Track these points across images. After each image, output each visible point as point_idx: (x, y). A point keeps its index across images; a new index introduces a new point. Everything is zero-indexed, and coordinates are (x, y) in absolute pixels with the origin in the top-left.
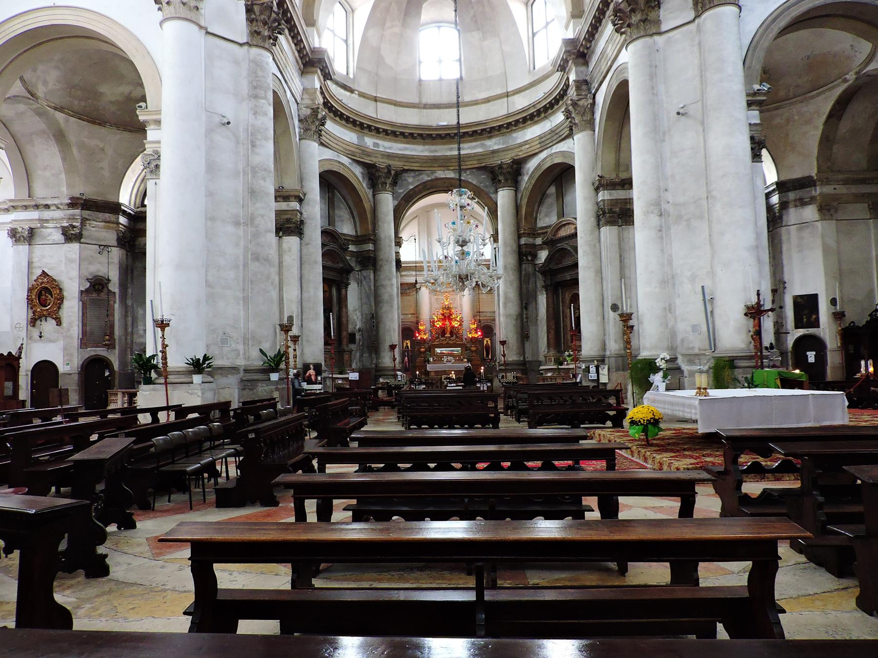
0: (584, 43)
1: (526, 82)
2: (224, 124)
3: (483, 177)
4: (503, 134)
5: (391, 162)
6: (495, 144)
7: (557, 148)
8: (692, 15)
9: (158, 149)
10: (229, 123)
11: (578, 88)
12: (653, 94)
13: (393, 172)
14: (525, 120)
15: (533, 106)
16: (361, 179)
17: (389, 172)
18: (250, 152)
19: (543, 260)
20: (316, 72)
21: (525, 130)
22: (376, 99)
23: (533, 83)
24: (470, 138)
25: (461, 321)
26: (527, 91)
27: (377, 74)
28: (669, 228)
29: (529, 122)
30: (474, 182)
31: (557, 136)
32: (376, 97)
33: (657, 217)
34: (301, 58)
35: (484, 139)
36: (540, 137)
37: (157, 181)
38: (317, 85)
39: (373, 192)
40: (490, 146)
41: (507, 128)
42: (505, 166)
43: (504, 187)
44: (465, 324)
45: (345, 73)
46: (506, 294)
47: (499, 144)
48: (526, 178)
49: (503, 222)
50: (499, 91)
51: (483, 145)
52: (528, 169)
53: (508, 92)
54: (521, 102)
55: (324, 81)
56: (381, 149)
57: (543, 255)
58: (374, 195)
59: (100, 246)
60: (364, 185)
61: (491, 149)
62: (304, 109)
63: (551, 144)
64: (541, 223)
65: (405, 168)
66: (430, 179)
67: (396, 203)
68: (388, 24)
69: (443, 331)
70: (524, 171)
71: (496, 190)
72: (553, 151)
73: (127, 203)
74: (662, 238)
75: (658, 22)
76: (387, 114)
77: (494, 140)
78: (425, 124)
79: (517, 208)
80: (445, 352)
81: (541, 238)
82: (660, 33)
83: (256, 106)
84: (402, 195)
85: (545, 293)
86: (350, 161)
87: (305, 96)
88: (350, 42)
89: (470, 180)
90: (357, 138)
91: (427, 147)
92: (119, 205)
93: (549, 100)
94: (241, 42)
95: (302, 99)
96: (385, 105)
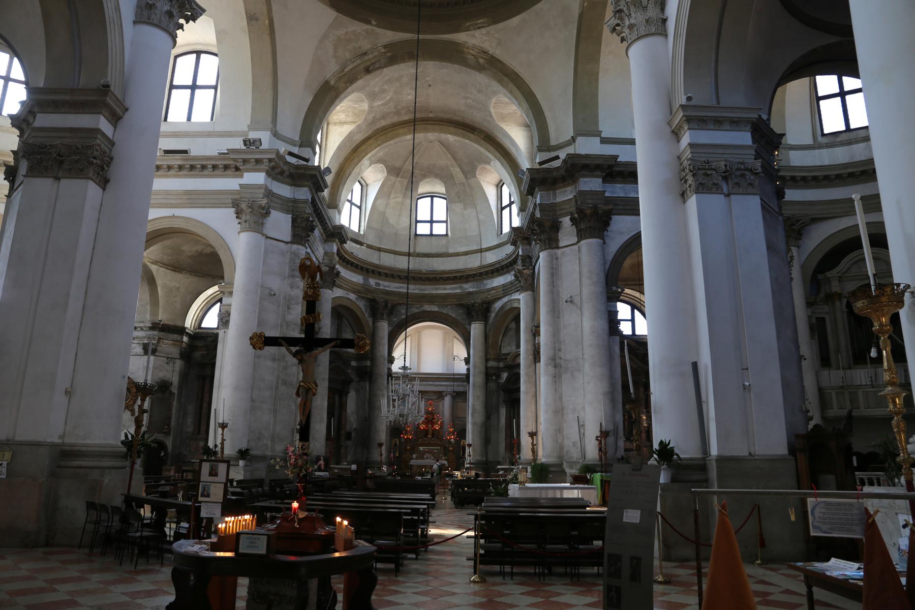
1: (495, 243)
2: (271, 295)
4: (477, 280)
5: (388, 298)
6: (470, 287)
7: (514, 296)
8: (576, 240)
9: (228, 310)
10: (274, 295)
11: (523, 261)
12: (553, 286)
13: (389, 305)
14: (492, 272)
16: (363, 310)
17: (386, 305)
18: (286, 312)
20: (335, 241)
21: (493, 279)
22: (379, 250)
23: (500, 245)
24: (452, 282)
26: (496, 250)
27: (382, 231)
28: (560, 376)
30: (453, 315)
31: (515, 287)
32: (380, 248)
33: (553, 368)
34: (325, 233)
35: (462, 283)
36: (503, 286)
37: (226, 330)
39: (373, 320)
40: (467, 289)
41: (480, 276)
43: (475, 321)
45: (357, 231)
47: (474, 287)
48: (493, 315)
49: (474, 349)
50: (475, 247)
51: (461, 288)
52: (495, 309)
53: (481, 249)
54: (491, 258)
55: (341, 245)
56: (381, 287)
57: (505, 375)
58: (374, 323)
60: (367, 315)
61: (467, 291)
62: (324, 267)
63: (511, 292)
64: (504, 351)
65: (400, 302)
66: (418, 311)
67: (391, 328)
68: (392, 196)
70: (492, 310)
71: (470, 322)
72: (512, 298)
74: (555, 382)
75: (557, 241)
76: (387, 260)
77: (469, 284)
78: (417, 269)
79: (486, 337)
82: (558, 248)
83: (292, 282)
84: (396, 323)
86: (356, 297)
88: (363, 208)
89: (450, 314)
90: (363, 279)
91: (418, 286)
93: (509, 260)
94: (286, 240)
95: (323, 259)
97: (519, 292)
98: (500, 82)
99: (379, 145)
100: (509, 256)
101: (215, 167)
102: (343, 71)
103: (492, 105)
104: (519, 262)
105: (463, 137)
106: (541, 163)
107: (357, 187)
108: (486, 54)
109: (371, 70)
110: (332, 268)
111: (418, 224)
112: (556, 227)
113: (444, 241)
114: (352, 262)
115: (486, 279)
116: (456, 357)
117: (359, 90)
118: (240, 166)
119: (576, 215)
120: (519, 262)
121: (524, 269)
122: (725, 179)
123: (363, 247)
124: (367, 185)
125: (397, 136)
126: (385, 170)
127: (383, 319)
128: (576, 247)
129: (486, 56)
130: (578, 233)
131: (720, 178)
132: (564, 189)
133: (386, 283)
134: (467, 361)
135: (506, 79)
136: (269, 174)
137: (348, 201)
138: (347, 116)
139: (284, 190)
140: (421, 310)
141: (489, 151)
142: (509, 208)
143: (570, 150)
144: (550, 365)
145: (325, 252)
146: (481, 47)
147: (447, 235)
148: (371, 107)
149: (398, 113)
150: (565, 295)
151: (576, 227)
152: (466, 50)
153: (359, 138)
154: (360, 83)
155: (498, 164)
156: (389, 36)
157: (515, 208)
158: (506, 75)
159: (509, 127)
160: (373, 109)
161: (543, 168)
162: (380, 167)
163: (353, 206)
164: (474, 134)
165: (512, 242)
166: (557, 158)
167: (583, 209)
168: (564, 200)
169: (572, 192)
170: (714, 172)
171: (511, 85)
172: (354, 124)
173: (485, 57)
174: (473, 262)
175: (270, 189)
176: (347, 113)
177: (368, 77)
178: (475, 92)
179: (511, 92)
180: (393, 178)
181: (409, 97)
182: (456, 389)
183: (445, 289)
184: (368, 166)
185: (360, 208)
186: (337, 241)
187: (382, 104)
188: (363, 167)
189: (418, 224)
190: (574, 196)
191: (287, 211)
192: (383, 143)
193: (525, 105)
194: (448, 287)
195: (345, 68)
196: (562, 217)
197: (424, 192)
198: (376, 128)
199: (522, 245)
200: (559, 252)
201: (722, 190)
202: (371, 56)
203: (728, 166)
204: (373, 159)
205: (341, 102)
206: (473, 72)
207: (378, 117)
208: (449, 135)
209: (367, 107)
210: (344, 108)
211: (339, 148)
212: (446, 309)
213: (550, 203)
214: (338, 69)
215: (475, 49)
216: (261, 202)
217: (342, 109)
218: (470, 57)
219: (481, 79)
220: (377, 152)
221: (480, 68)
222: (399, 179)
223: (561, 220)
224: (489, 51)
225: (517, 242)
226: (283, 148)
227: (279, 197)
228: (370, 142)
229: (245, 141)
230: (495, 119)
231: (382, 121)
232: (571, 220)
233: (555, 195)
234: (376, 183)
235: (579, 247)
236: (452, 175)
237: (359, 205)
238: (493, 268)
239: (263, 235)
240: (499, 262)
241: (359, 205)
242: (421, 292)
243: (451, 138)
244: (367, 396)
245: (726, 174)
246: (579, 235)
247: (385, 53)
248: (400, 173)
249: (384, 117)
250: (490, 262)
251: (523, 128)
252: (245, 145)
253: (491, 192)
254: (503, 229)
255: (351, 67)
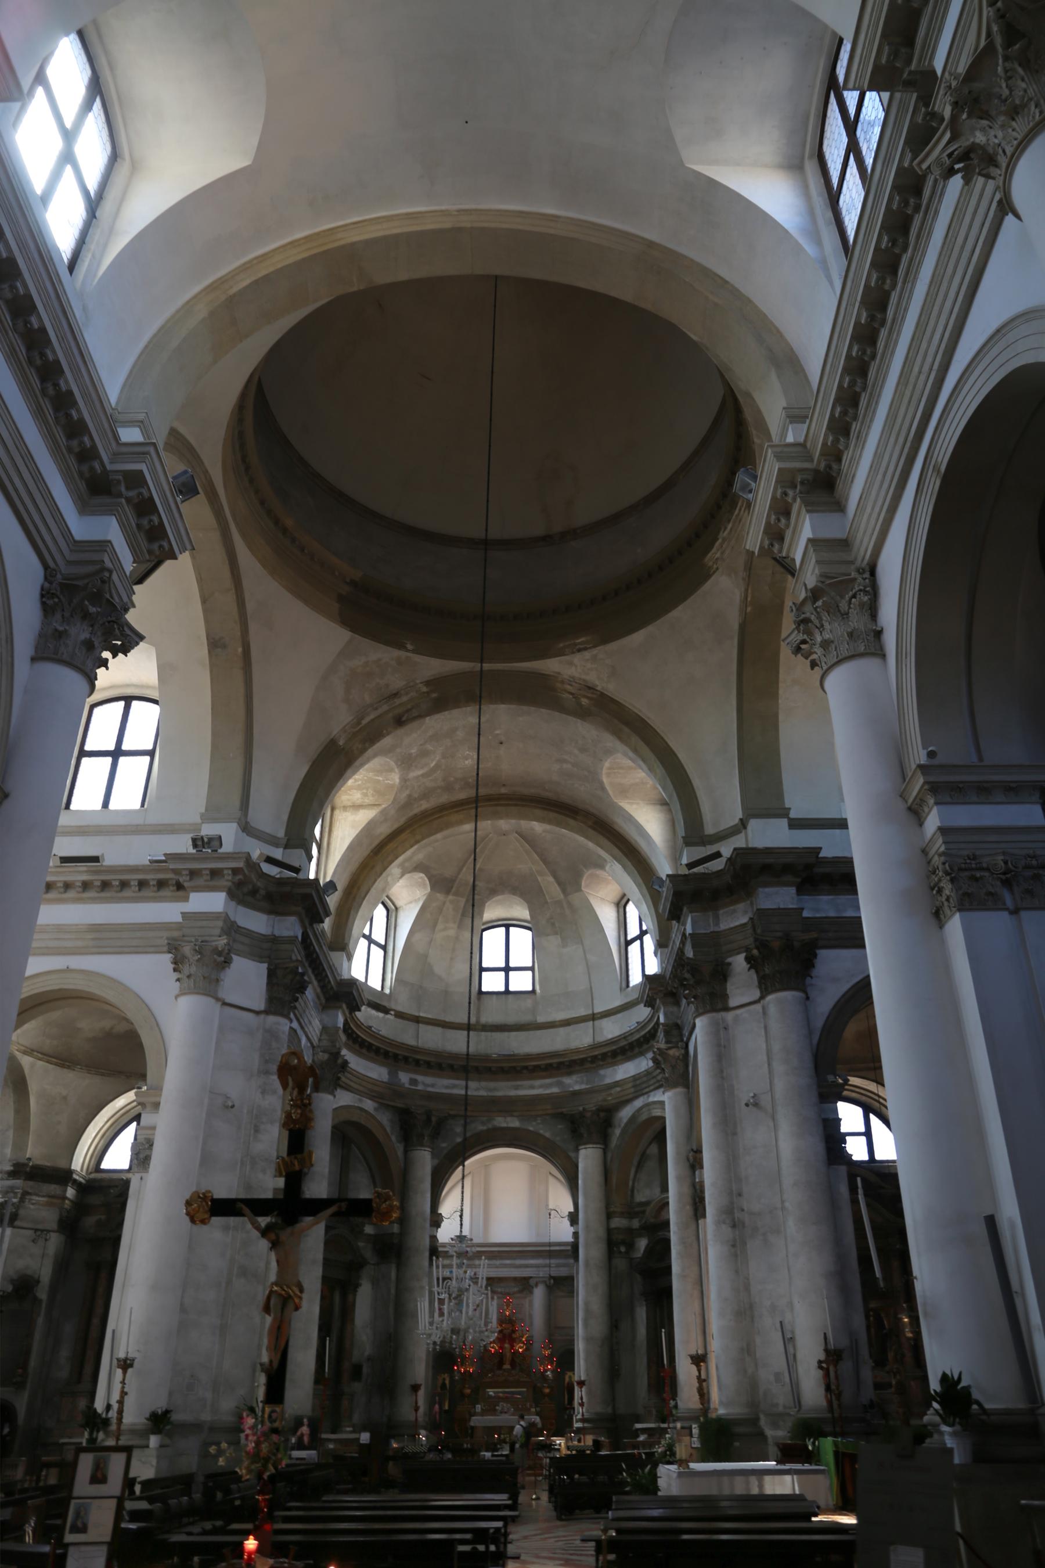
0: (670, 982)
1: (617, 1003)
3: (560, 1127)
6: (577, 1082)
8: (757, 994)
9: (151, 1137)
10: (233, 1107)
11: (667, 1033)
12: (723, 1078)
13: (434, 1119)
15: (625, 1038)
17: (429, 1119)
18: (251, 1139)
19: (642, 1251)
21: (616, 1067)
22: (417, 1020)
25: (529, 1344)
26: (619, 1015)
28: (744, 1243)
29: (619, 1058)
30: (547, 1135)
33: (730, 1229)
36: (635, 1078)
38: (341, 1020)
41: (592, 1062)
42: (588, 1115)
44: (537, 1346)
45: (379, 989)
46: (587, 1304)
47: (582, 1083)
48: (617, 1132)
50: (583, 1012)
51: (559, 1084)
53: (594, 1014)
54: (611, 1029)
55: (350, 1013)
56: (420, 1087)
57: (642, 1244)
59: (36, 1230)
61: (571, 1089)
62: (321, 1054)
63: (647, 1090)
64: (640, 1198)
65: (452, 1113)
66: (485, 1128)
67: (436, 1161)
68: (440, 926)
69: (500, 1359)
73: (79, 1169)
74: (736, 1255)
75: (725, 997)
76: (431, 1039)
77: (575, 1077)
80: (501, 1395)
81: (637, 1220)
82: (727, 1009)
85: (644, 1303)
87: (324, 1037)
88: (390, 948)
89: (541, 1132)
91: (484, 1084)
92: (70, 1172)
93: (643, 1033)
94: (256, 1008)
95: (320, 1040)
96: (430, 1027)
97: (662, 1090)
98: (618, 735)
99: (417, 842)
100: (642, 1026)
101: (142, 884)
102: (359, 723)
103: (604, 771)
104: (661, 1035)
105: (558, 824)
106: (690, 866)
107: (380, 913)
108: (592, 691)
109: (404, 721)
110: (336, 1055)
111: (484, 974)
112: (722, 973)
113: (529, 1002)
114: (370, 1043)
115: (602, 1067)
116: (553, 1212)
117: (385, 752)
118: (184, 881)
119: (755, 952)
120: (661, 1035)
121: (669, 1048)
122: (1007, 883)
123: (389, 1016)
124: (396, 909)
125: (448, 825)
126: (428, 882)
127: (422, 1145)
128: (758, 1007)
129: (593, 693)
130: (760, 983)
131: (999, 883)
132: (732, 908)
133: (429, 1080)
134: (573, 1218)
135: (626, 730)
136: (231, 895)
137: (364, 936)
138: (365, 795)
139: (256, 922)
140: (490, 1126)
141: (602, 848)
142: (638, 942)
143: (739, 842)
144: (724, 1223)
145: (323, 1028)
146: (584, 680)
147: (533, 991)
148: (404, 780)
149: (448, 788)
150: (744, 1094)
151: (757, 972)
152: (559, 685)
153: (385, 830)
154: (387, 741)
155: (618, 867)
156: (434, 666)
157: (648, 940)
158: (627, 724)
159: (635, 806)
160: (408, 783)
161: (695, 874)
162: (421, 878)
163: (372, 945)
164: (575, 819)
165: (646, 1001)
166: (718, 855)
167: (767, 941)
168: (732, 925)
169: (746, 912)
170: (987, 874)
171: (635, 739)
172: (376, 808)
173: (590, 695)
174: (581, 1038)
175: (232, 919)
176: (365, 791)
177: (401, 731)
178: (576, 752)
179: (635, 751)
180: (440, 896)
181: (467, 762)
182: (555, 1272)
183: (532, 1087)
184: (399, 876)
185: (384, 948)
186: (344, 1006)
187: (423, 775)
188: (389, 879)
189: (484, 974)
190: (751, 919)
191: (259, 958)
192: (423, 839)
193: (660, 770)
194: (538, 1082)
195: (362, 718)
196: (731, 956)
197: (494, 918)
198: (411, 814)
199: (664, 1006)
200: (729, 1016)
201: (1004, 904)
202: (405, 699)
203: (1009, 863)
204: (407, 864)
205: (354, 773)
206: (570, 718)
207: (416, 795)
208: (535, 823)
209: (397, 781)
210: (360, 782)
211: (351, 848)
212: (534, 1123)
213: (709, 932)
214: (353, 720)
215: (574, 684)
216: (216, 943)
217: (357, 783)
218: (566, 695)
219: (586, 731)
220: (414, 853)
221: (582, 714)
222: (451, 897)
223: (729, 960)
224: (597, 686)
225: (655, 1000)
226: (257, 850)
227: (249, 933)
228: (403, 836)
229: (194, 841)
230: (611, 793)
231: (422, 802)
232: (748, 959)
233: (717, 918)
234: (412, 905)
235: (764, 1008)
236: (541, 887)
237: (383, 943)
238: (614, 1047)
239: (218, 999)
240: (624, 1037)
241: (383, 943)
242: (490, 1094)
243: (538, 827)
244: (393, 1291)
245: (1008, 876)
246: (763, 987)
247: (428, 693)
248: (452, 887)
249: (425, 795)
250: (610, 1036)
251: (659, 807)
252: (195, 846)
253: (607, 916)
254: (631, 979)
255: (372, 717)
